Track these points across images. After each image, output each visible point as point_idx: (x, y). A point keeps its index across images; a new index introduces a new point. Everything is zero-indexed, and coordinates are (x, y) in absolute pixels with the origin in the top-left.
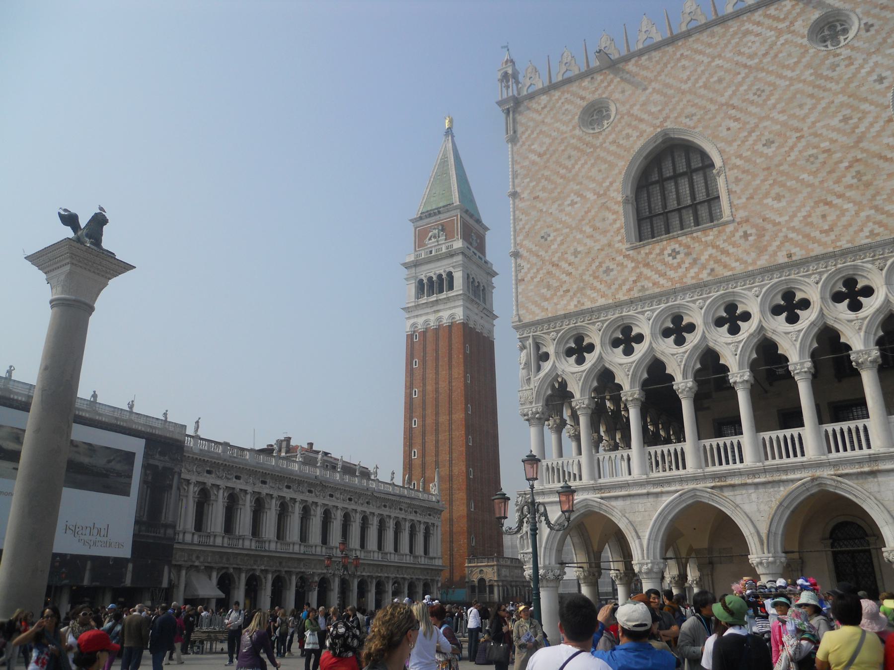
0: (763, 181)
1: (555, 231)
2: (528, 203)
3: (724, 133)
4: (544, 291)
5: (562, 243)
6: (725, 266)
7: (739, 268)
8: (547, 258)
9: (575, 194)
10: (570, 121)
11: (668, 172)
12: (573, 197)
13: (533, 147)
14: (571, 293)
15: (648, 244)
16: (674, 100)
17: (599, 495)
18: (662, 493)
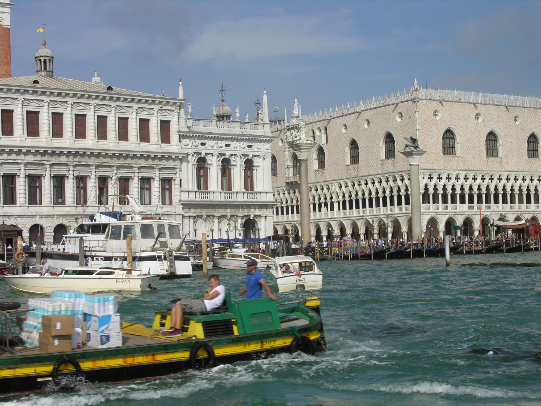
11: (445, 136)
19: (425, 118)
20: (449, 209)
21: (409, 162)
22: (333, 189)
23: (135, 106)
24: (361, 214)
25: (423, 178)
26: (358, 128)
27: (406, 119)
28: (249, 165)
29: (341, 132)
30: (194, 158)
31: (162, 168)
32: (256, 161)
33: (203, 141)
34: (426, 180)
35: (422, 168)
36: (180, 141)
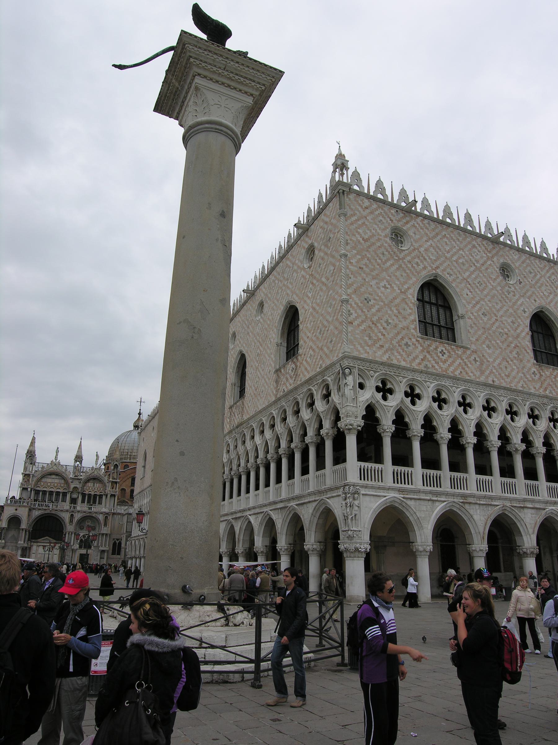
0: (483, 334)
1: (375, 299)
2: (356, 269)
3: (465, 296)
4: (367, 338)
5: (378, 311)
6: (467, 373)
7: (473, 378)
8: (368, 316)
9: (387, 282)
13: (359, 230)
14: (384, 349)
15: (430, 339)
16: (442, 259)
17: (403, 496)
18: (437, 501)
19: (366, 237)
20: (446, 486)
26: (248, 327)
27: (320, 250)
34: (369, 395)
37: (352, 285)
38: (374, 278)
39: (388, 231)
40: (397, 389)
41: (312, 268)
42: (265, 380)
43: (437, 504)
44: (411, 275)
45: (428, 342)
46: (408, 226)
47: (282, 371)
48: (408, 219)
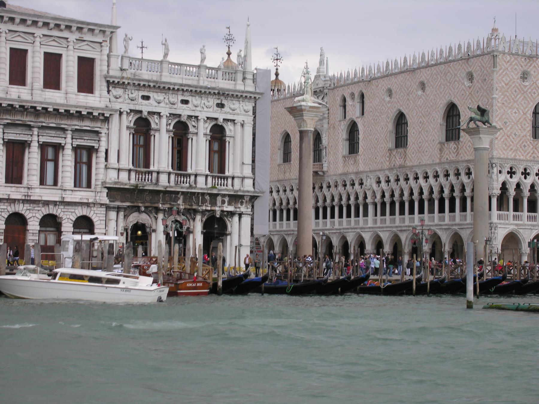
1: (509, 122)
4: (504, 146)
5: (511, 128)
10: (517, 74)
12: (515, 110)
14: (513, 150)
19: (507, 82)
21: (473, 144)
22: (368, 184)
23: (39, 32)
24: (407, 223)
25: (500, 172)
26: (408, 94)
27: (478, 82)
28: (218, 135)
29: (383, 99)
30: (130, 118)
31: (77, 130)
32: (229, 128)
33: (146, 94)
35: (498, 156)
36: (109, 91)
37: (498, 115)
38: (510, 108)
39: (519, 75)
40: (518, 172)
41: (471, 89)
42: (429, 144)
43: (533, 230)
44: (530, 101)
45: (536, 143)
46: (531, 67)
47: (446, 145)
48: (531, 62)
